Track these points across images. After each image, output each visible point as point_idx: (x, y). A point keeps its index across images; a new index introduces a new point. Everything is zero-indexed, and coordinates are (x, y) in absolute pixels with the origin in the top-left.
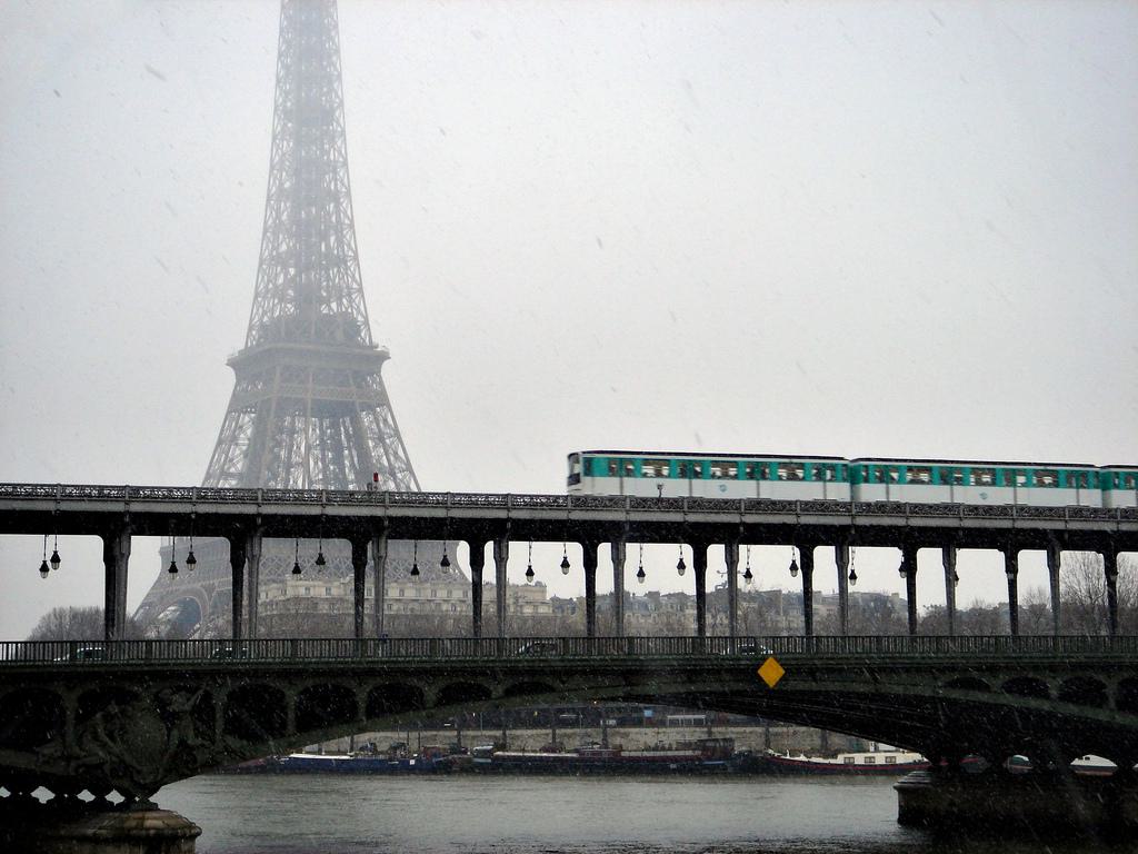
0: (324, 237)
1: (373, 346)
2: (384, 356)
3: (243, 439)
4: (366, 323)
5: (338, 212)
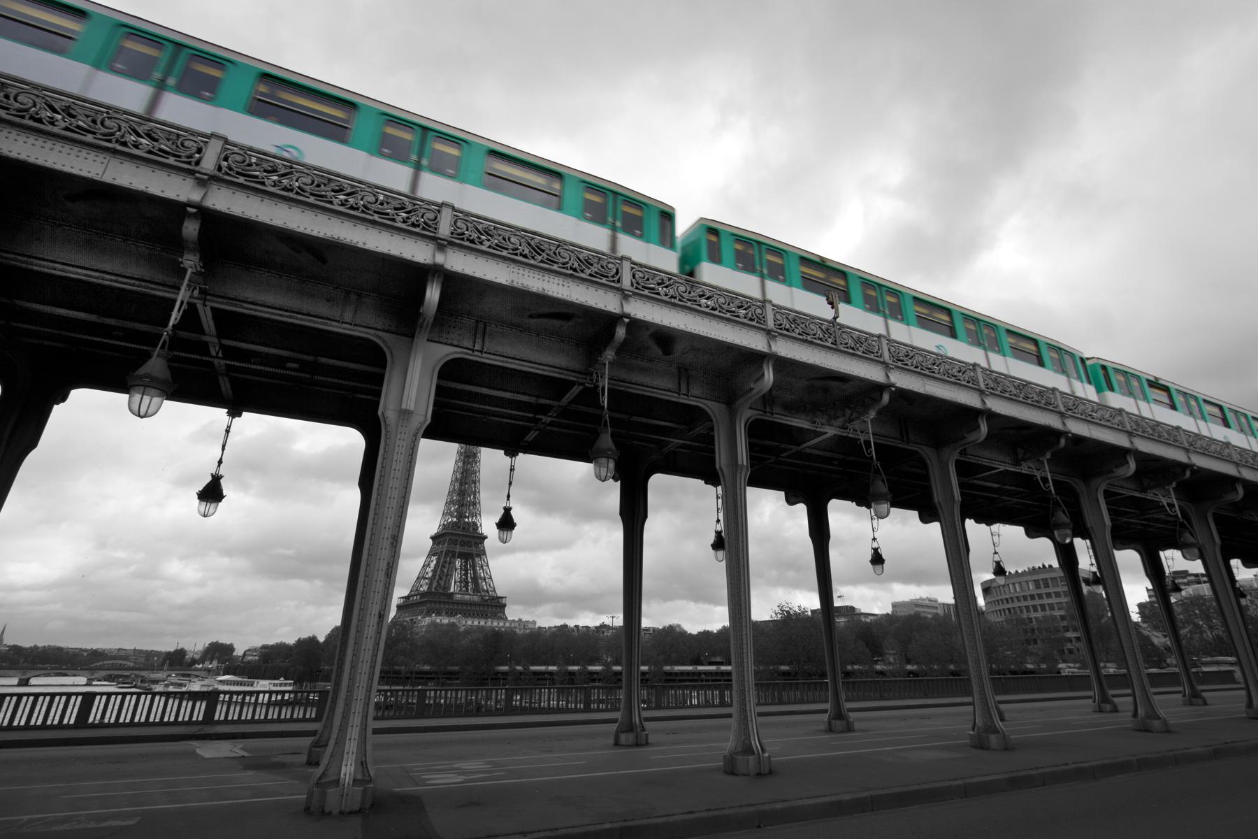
0: (470, 497)
1: (482, 534)
2: (486, 537)
3: (432, 565)
4: (481, 525)
5: (475, 487)
